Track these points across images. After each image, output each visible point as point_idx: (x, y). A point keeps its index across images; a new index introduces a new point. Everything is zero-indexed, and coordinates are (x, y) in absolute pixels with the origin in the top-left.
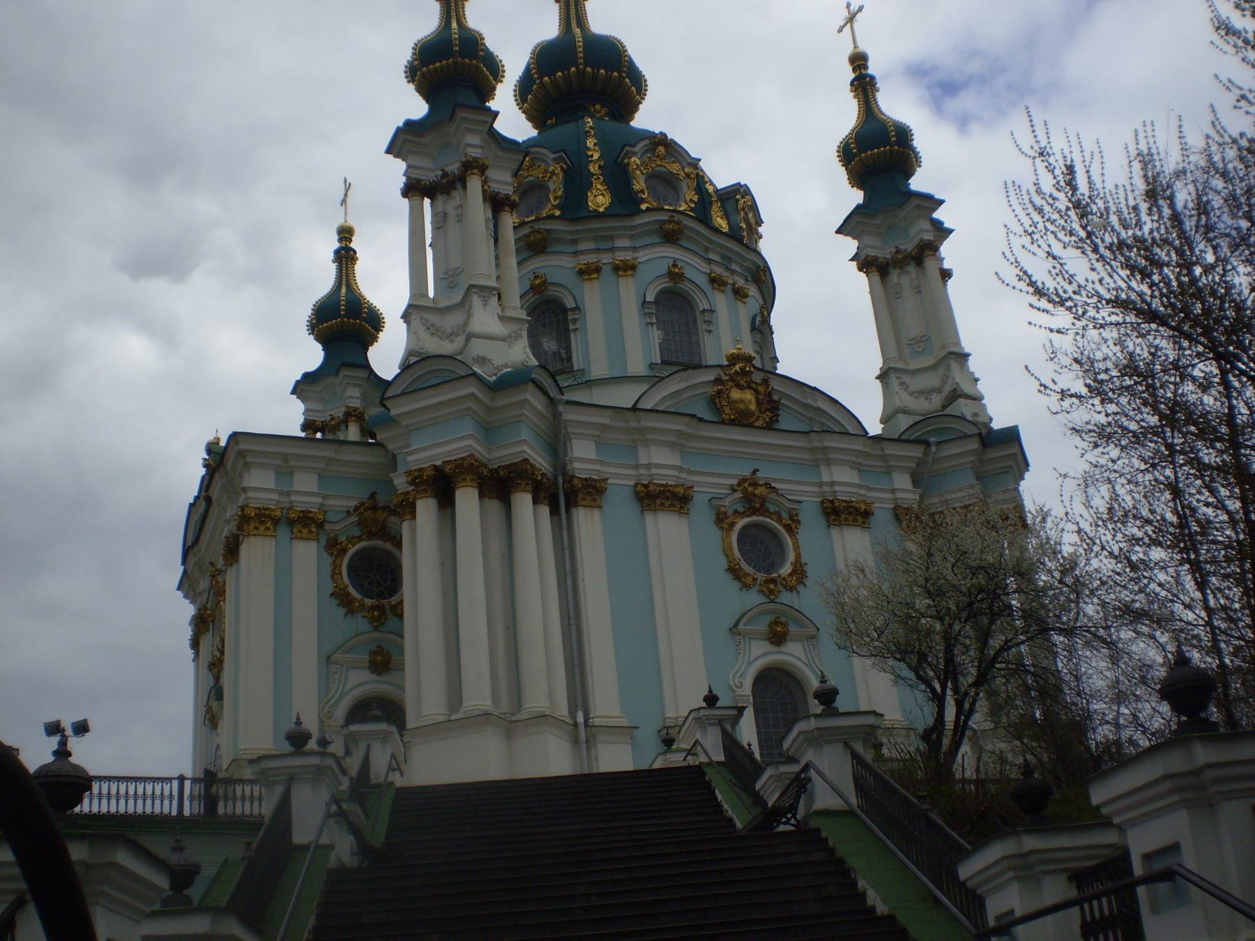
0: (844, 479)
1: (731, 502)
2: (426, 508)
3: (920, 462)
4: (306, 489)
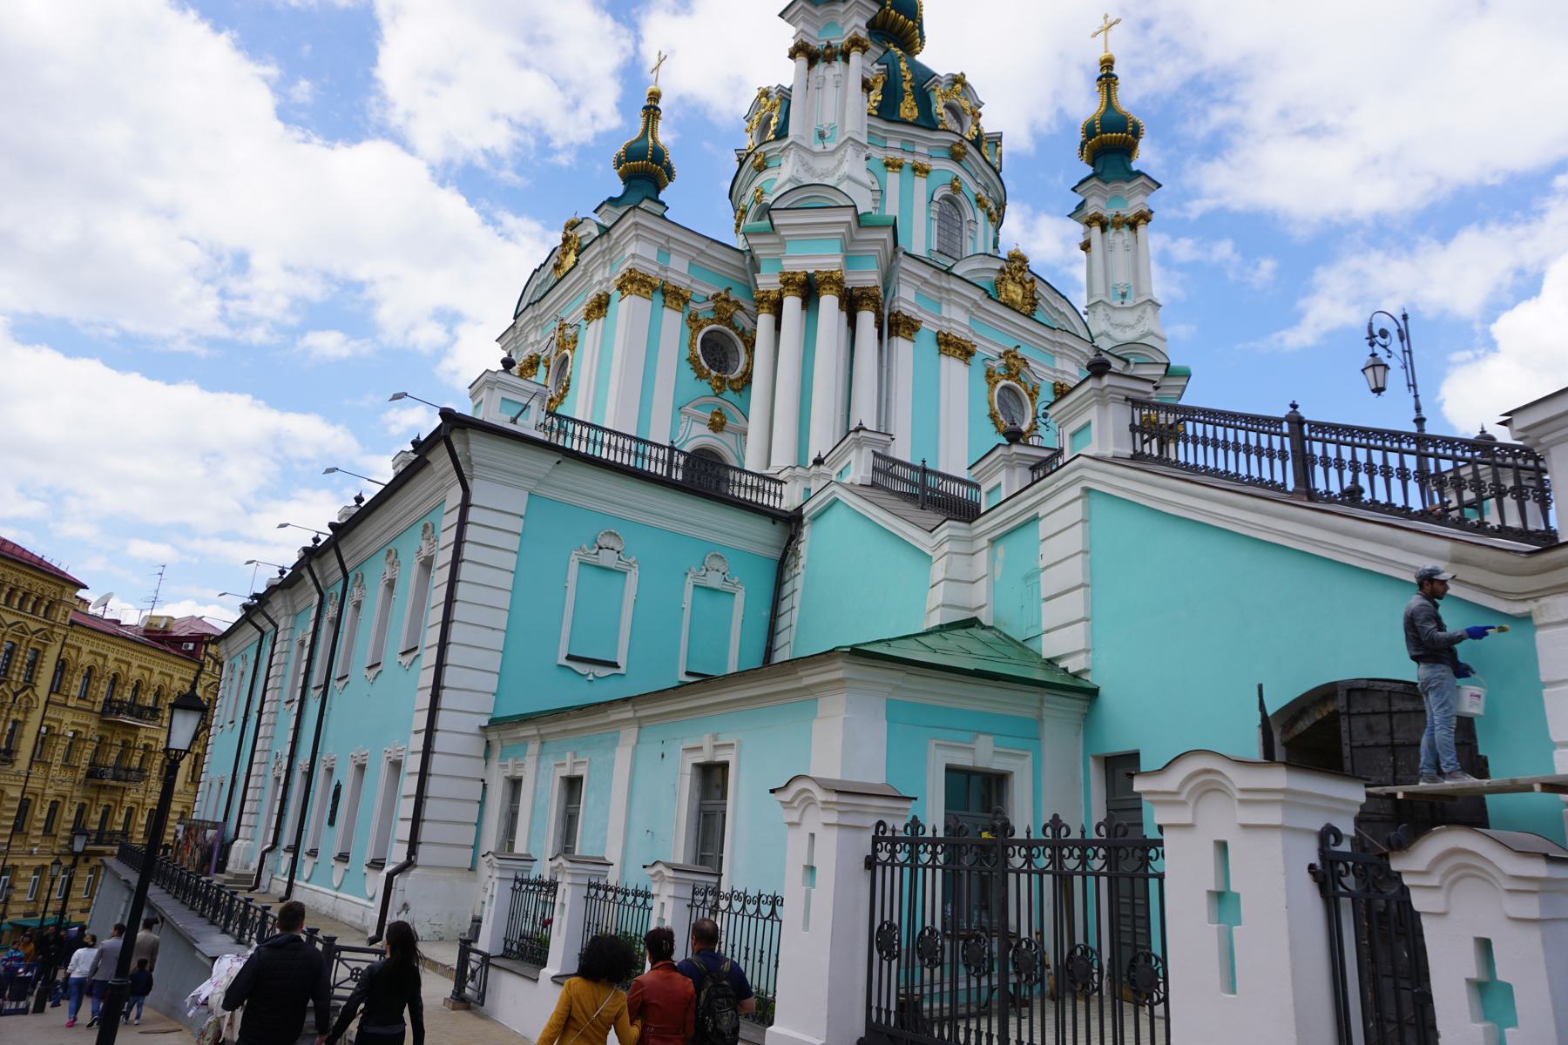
1: (998, 365)
2: (792, 304)
4: (678, 271)
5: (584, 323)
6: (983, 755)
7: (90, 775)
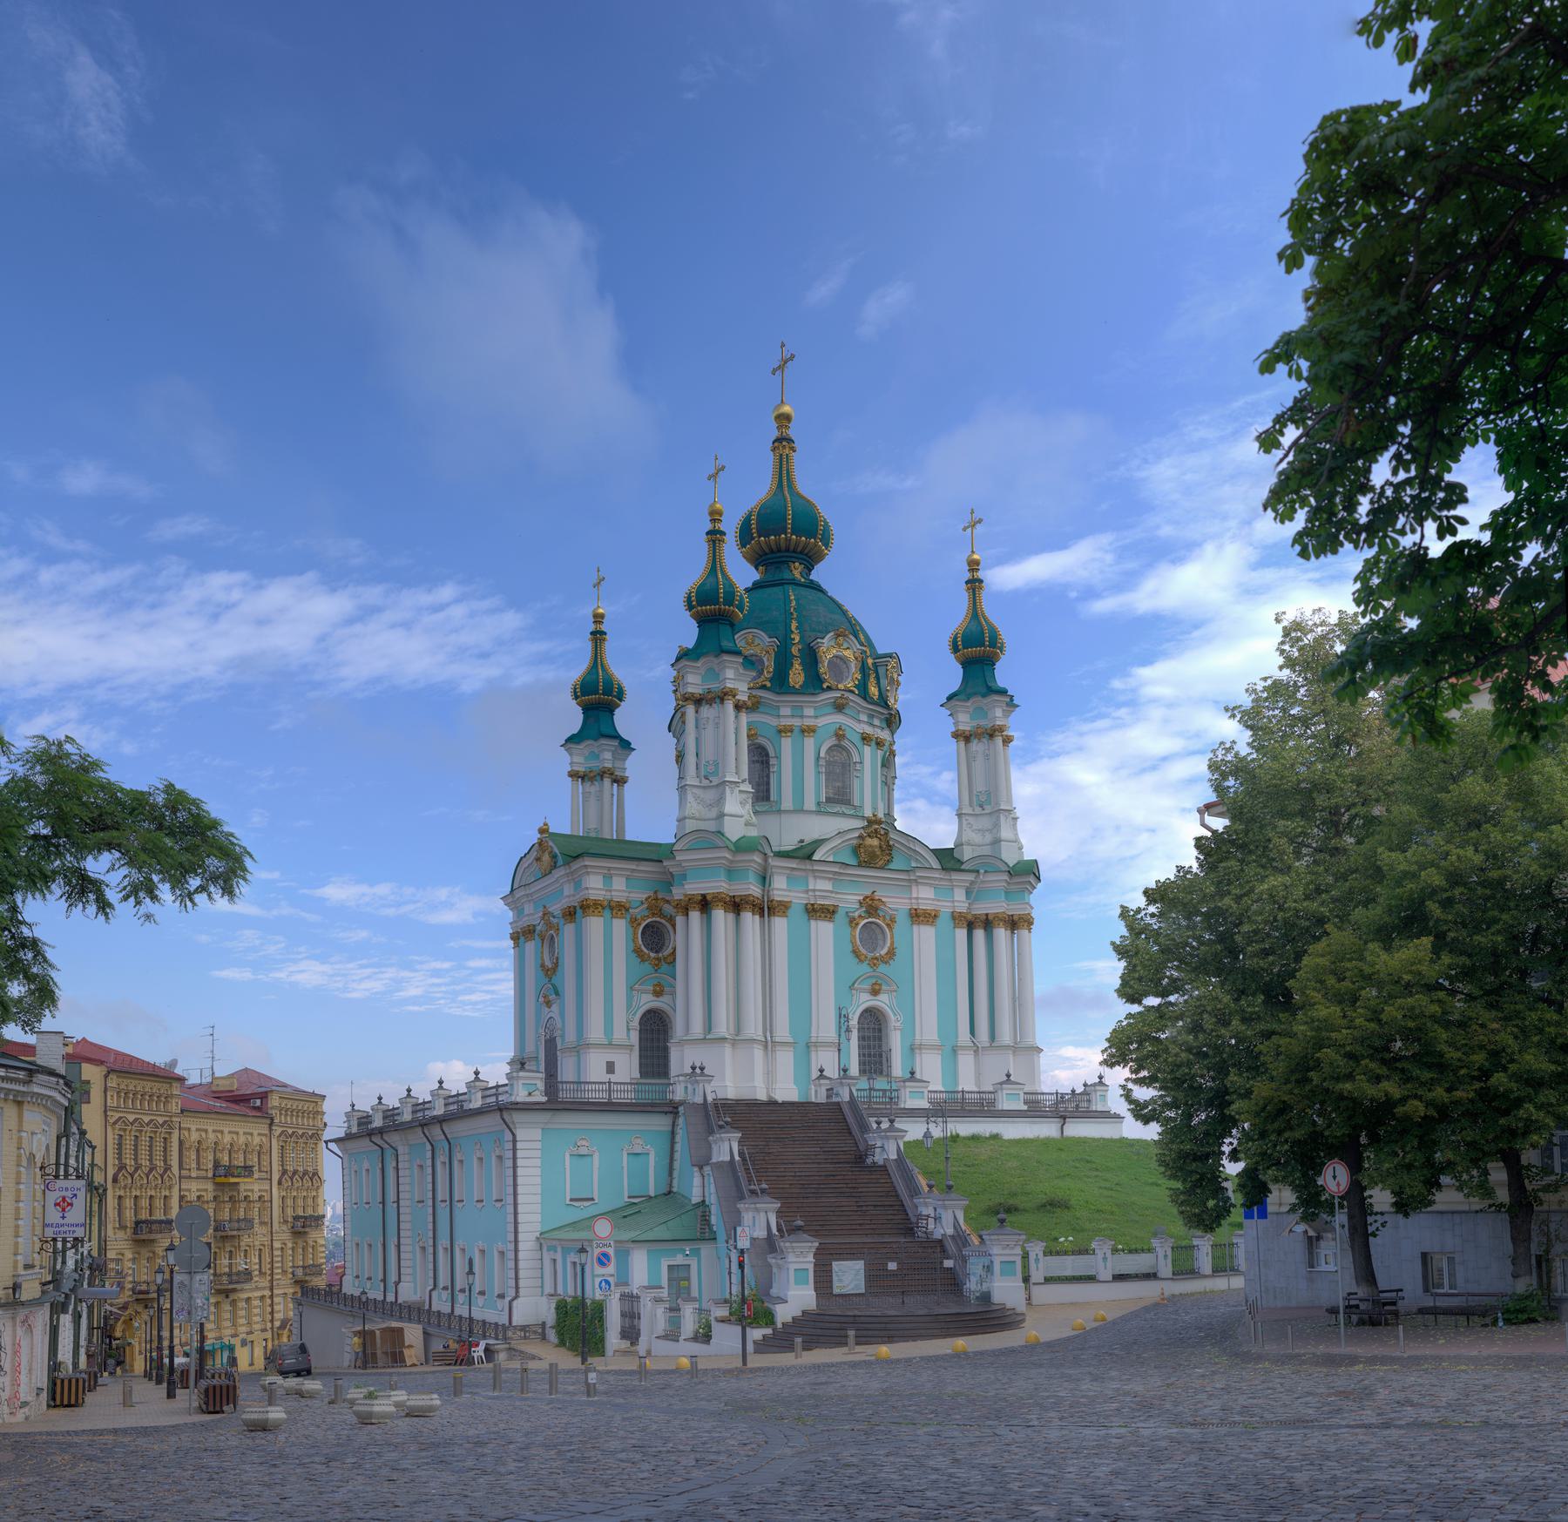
0: (925, 896)
3: (972, 883)
4: (620, 888)
5: (562, 921)
6: (679, 1260)
7: (216, 1230)
